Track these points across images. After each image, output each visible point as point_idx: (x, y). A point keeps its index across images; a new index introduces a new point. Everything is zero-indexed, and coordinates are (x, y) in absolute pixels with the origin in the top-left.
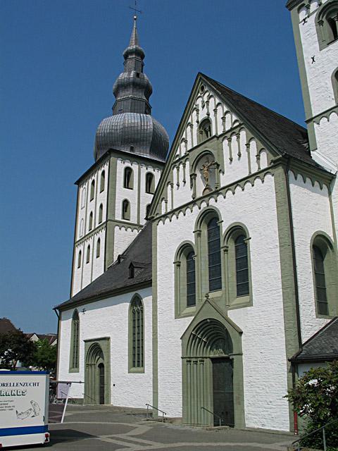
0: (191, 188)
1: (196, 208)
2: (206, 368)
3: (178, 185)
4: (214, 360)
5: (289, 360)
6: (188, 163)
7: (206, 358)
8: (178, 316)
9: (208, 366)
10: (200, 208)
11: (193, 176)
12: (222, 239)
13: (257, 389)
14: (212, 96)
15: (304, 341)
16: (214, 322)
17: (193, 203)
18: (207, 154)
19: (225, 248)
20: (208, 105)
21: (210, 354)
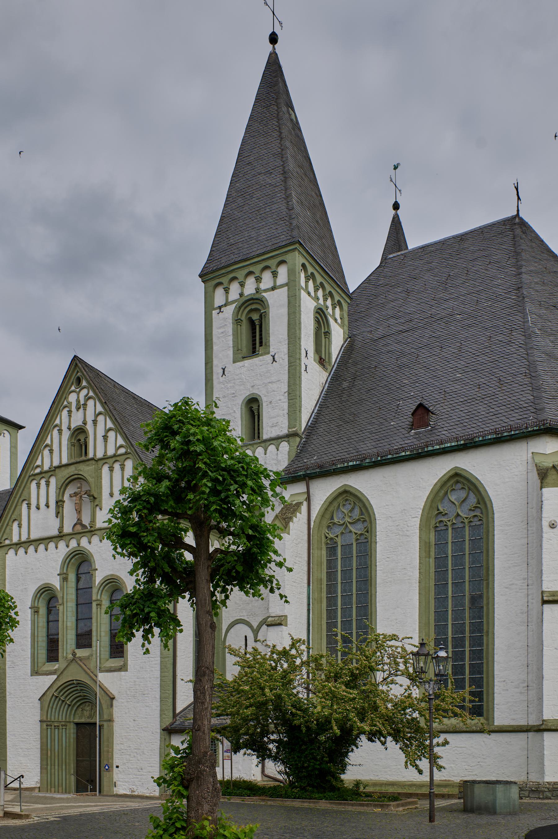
0: (57, 517)
1: (62, 544)
2: (69, 734)
3: (38, 508)
4: (77, 724)
5: (163, 730)
6: (53, 480)
7: (70, 722)
8: (35, 672)
9: (72, 731)
10: (68, 546)
11: (60, 503)
12: (95, 591)
13: (128, 757)
14: (90, 398)
15: (178, 710)
16: (80, 683)
17: (61, 536)
18: (80, 478)
19: (99, 602)
21: (74, 719)
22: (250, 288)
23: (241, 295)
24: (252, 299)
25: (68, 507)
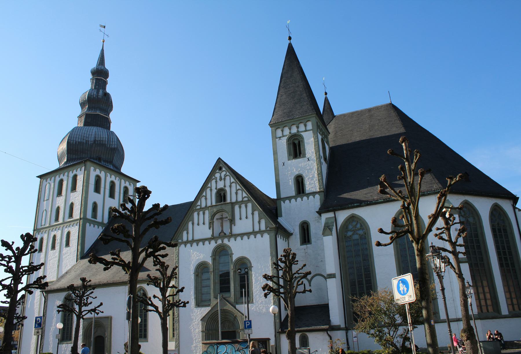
1: (213, 242)
20: (225, 181)
22: (294, 130)
23: (290, 133)
24: (295, 135)
25: (217, 224)
